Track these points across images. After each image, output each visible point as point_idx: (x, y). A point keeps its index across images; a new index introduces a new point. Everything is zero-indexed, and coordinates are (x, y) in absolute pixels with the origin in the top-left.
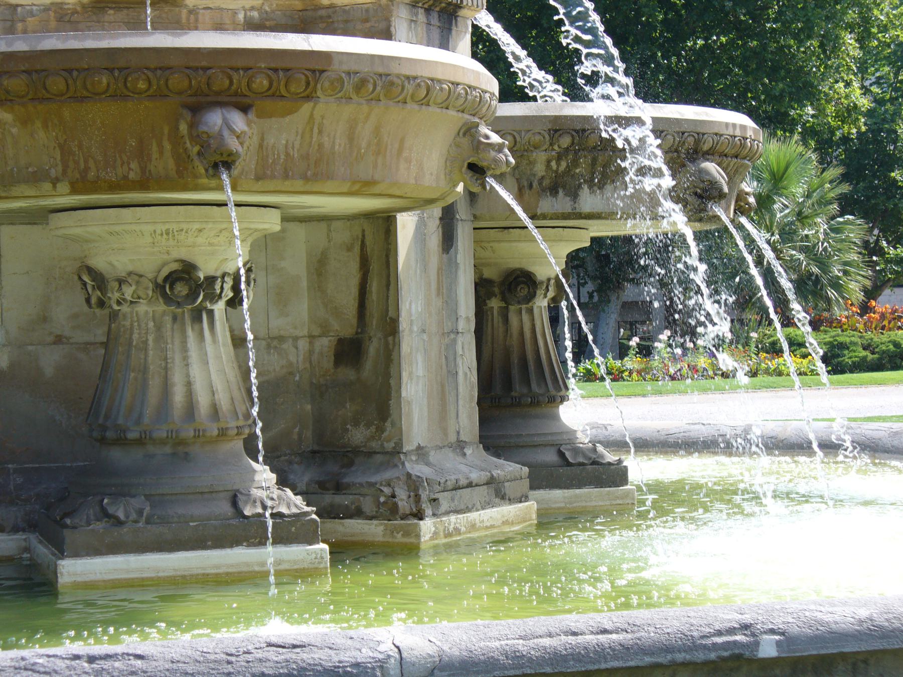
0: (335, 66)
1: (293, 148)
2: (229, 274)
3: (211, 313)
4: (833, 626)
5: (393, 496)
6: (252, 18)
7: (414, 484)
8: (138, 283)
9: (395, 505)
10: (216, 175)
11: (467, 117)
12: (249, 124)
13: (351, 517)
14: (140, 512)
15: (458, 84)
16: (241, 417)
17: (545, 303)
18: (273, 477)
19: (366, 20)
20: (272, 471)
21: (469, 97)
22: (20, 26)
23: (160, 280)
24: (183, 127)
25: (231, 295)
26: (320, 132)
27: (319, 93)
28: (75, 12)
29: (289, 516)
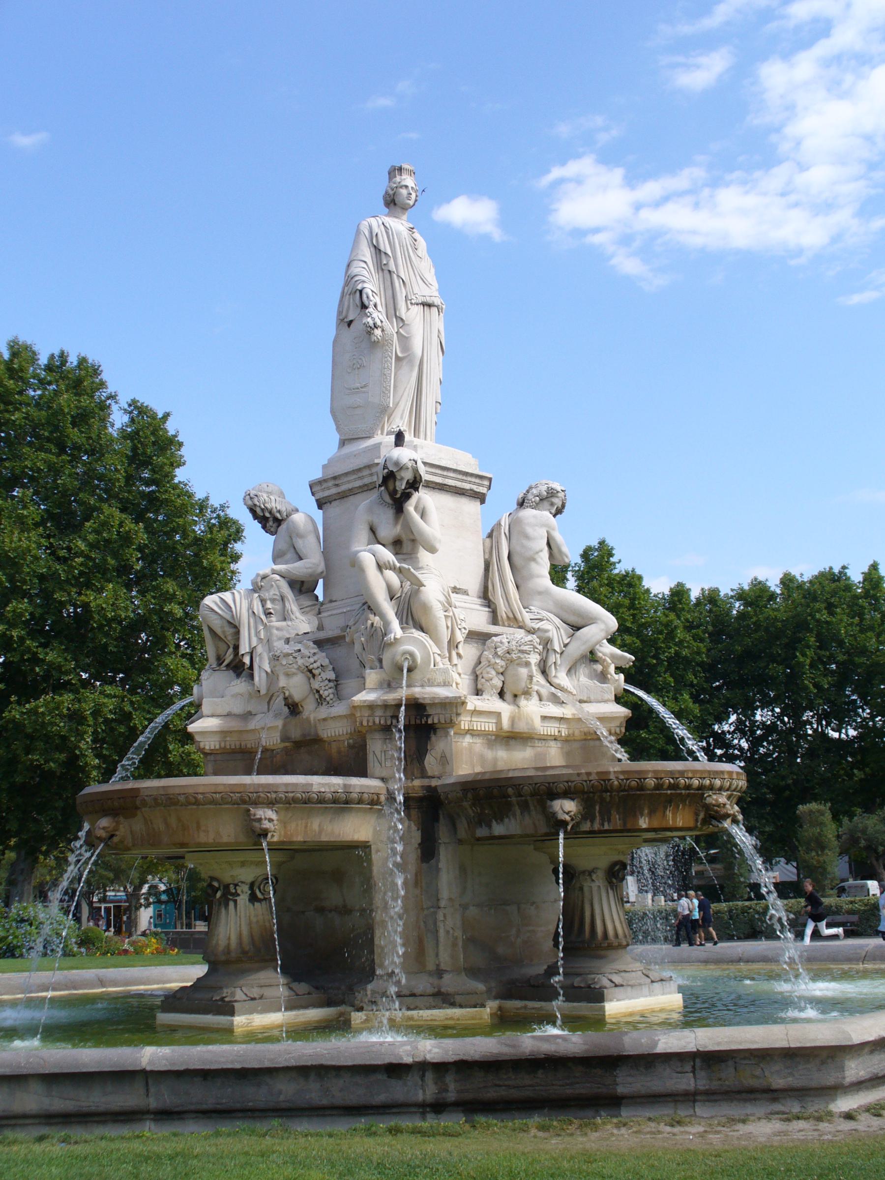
0: (142, 794)
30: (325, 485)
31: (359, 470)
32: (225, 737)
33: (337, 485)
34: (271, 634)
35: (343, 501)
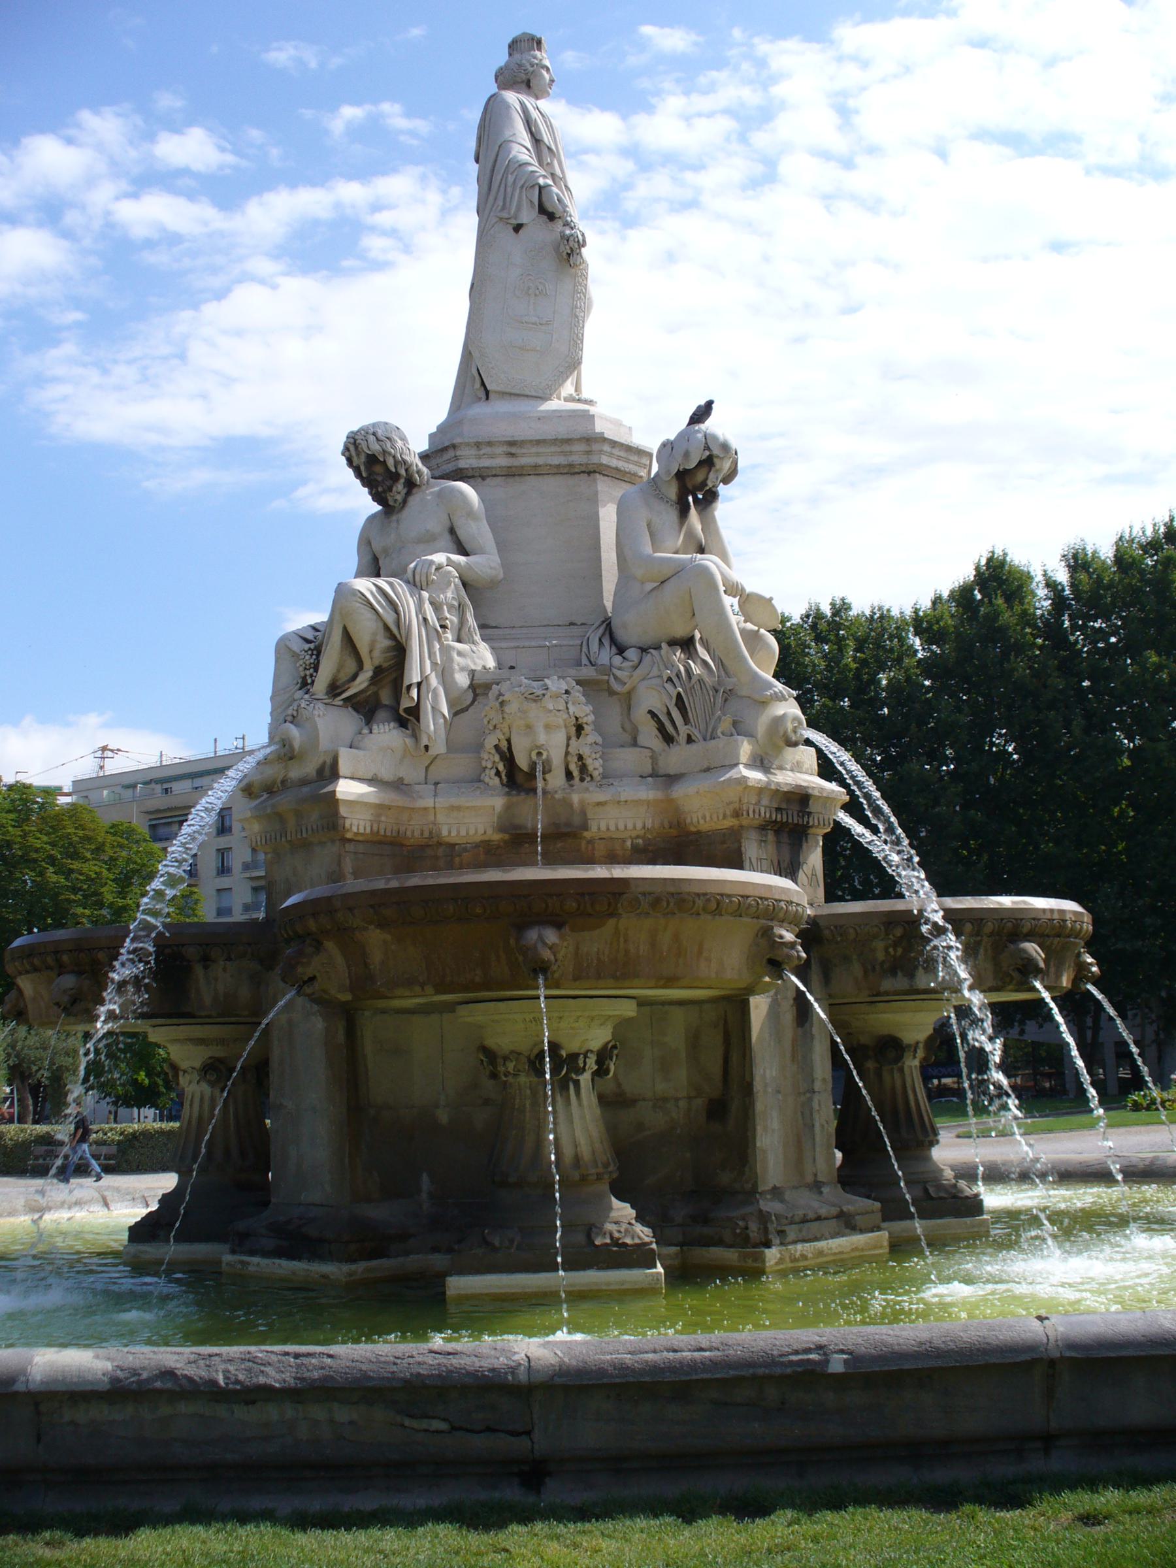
1: (604, 954)
2: (592, 1051)
3: (577, 1084)
4: (896, 1347)
5: (747, 1228)
6: (637, 844)
7: (764, 1218)
8: (517, 1059)
9: (748, 1236)
10: (536, 979)
11: (763, 922)
12: (562, 938)
13: (715, 1245)
14: (512, 1241)
15: (748, 897)
16: (600, 1165)
17: (916, 1063)
18: (633, 1213)
19: (724, 842)
20: (632, 1207)
21: (761, 907)
22: (457, 860)
23: (532, 1057)
24: (512, 942)
25: (596, 1067)
26: (626, 941)
27: (620, 911)
28: (498, 847)
29: (632, 1246)
30: (486, 450)
31: (568, 441)
32: (379, 815)
33: (512, 455)
34: (451, 660)
35: (511, 480)
